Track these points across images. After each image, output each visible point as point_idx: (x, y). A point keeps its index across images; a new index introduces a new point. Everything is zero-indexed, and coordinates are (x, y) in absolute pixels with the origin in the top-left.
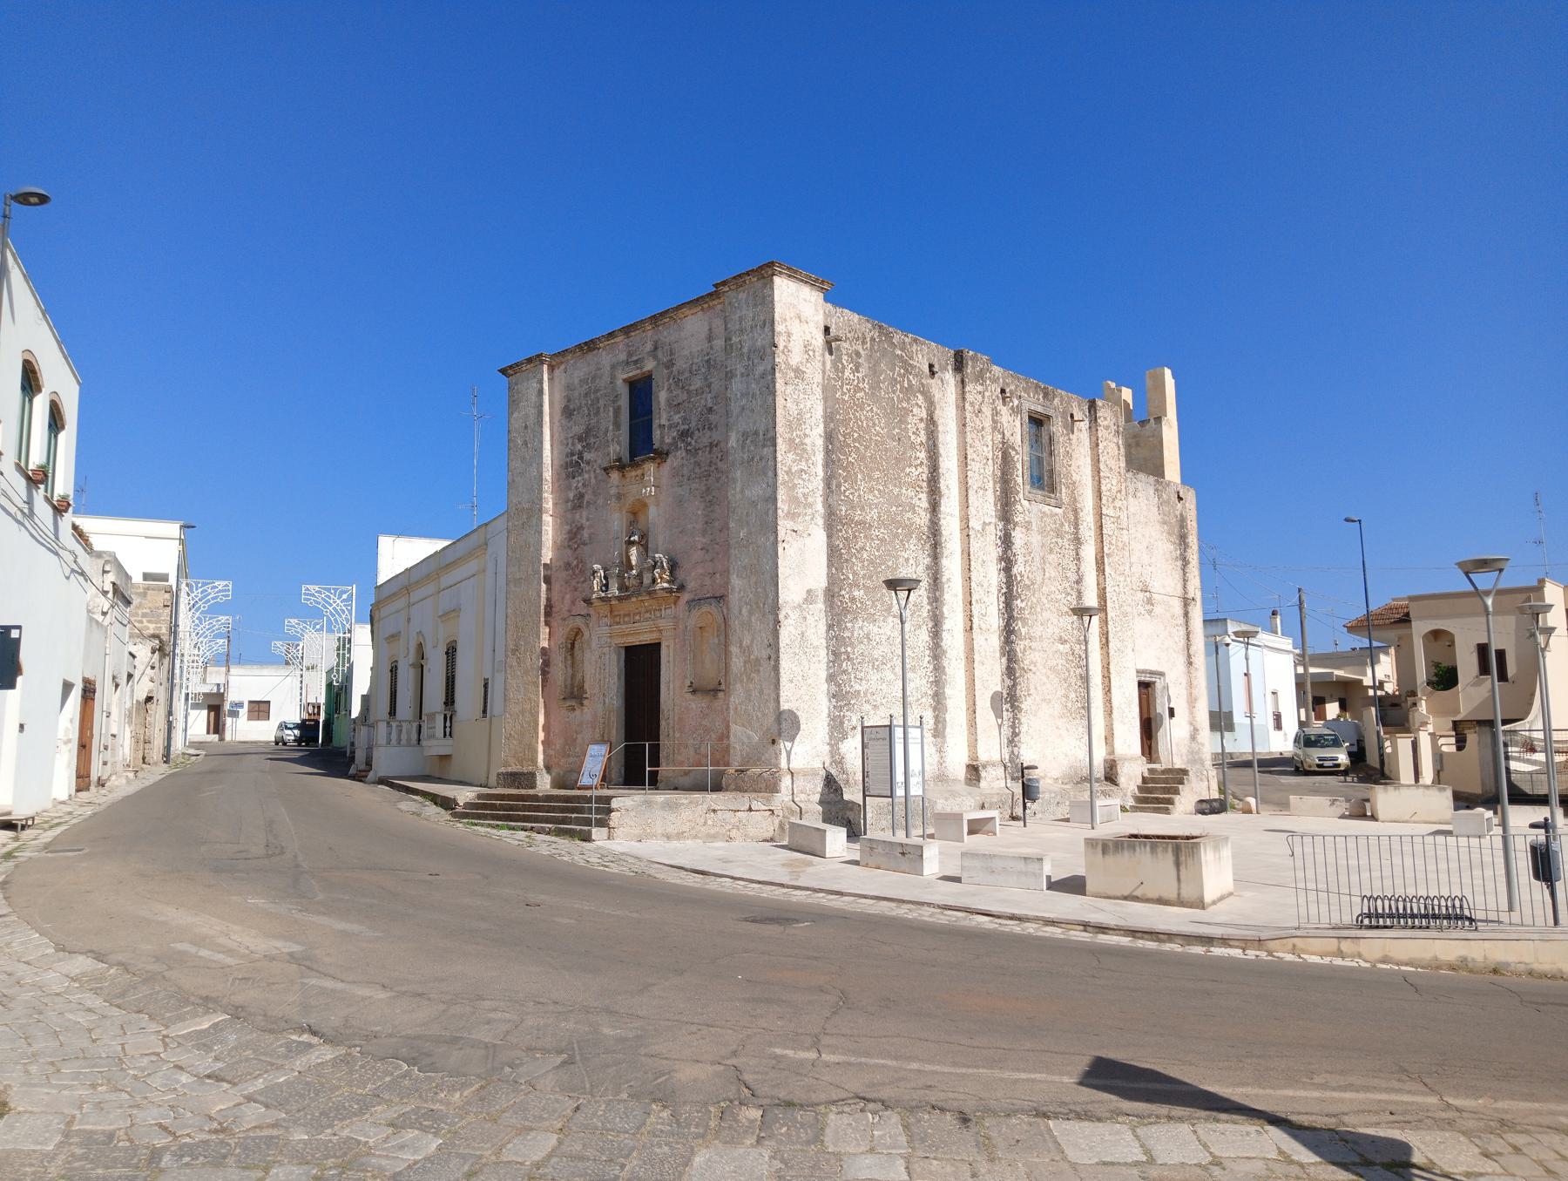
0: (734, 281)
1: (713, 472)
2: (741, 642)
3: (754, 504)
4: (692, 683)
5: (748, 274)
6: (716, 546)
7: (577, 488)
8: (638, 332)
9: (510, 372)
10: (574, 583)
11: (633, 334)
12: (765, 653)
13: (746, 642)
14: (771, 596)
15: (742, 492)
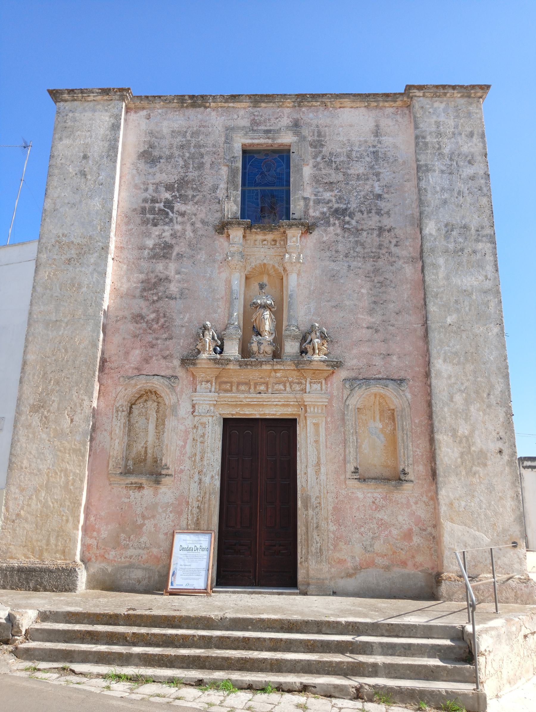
0: (435, 90)
1: (383, 254)
2: (454, 432)
3: (467, 293)
4: (356, 468)
5: (454, 87)
6: (391, 328)
7: (160, 236)
8: (271, 104)
9: (66, 96)
10: (150, 338)
11: (263, 105)
12: (493, 446)
13: (463, 429)
14: (499, 388)
15: (447, 278)
